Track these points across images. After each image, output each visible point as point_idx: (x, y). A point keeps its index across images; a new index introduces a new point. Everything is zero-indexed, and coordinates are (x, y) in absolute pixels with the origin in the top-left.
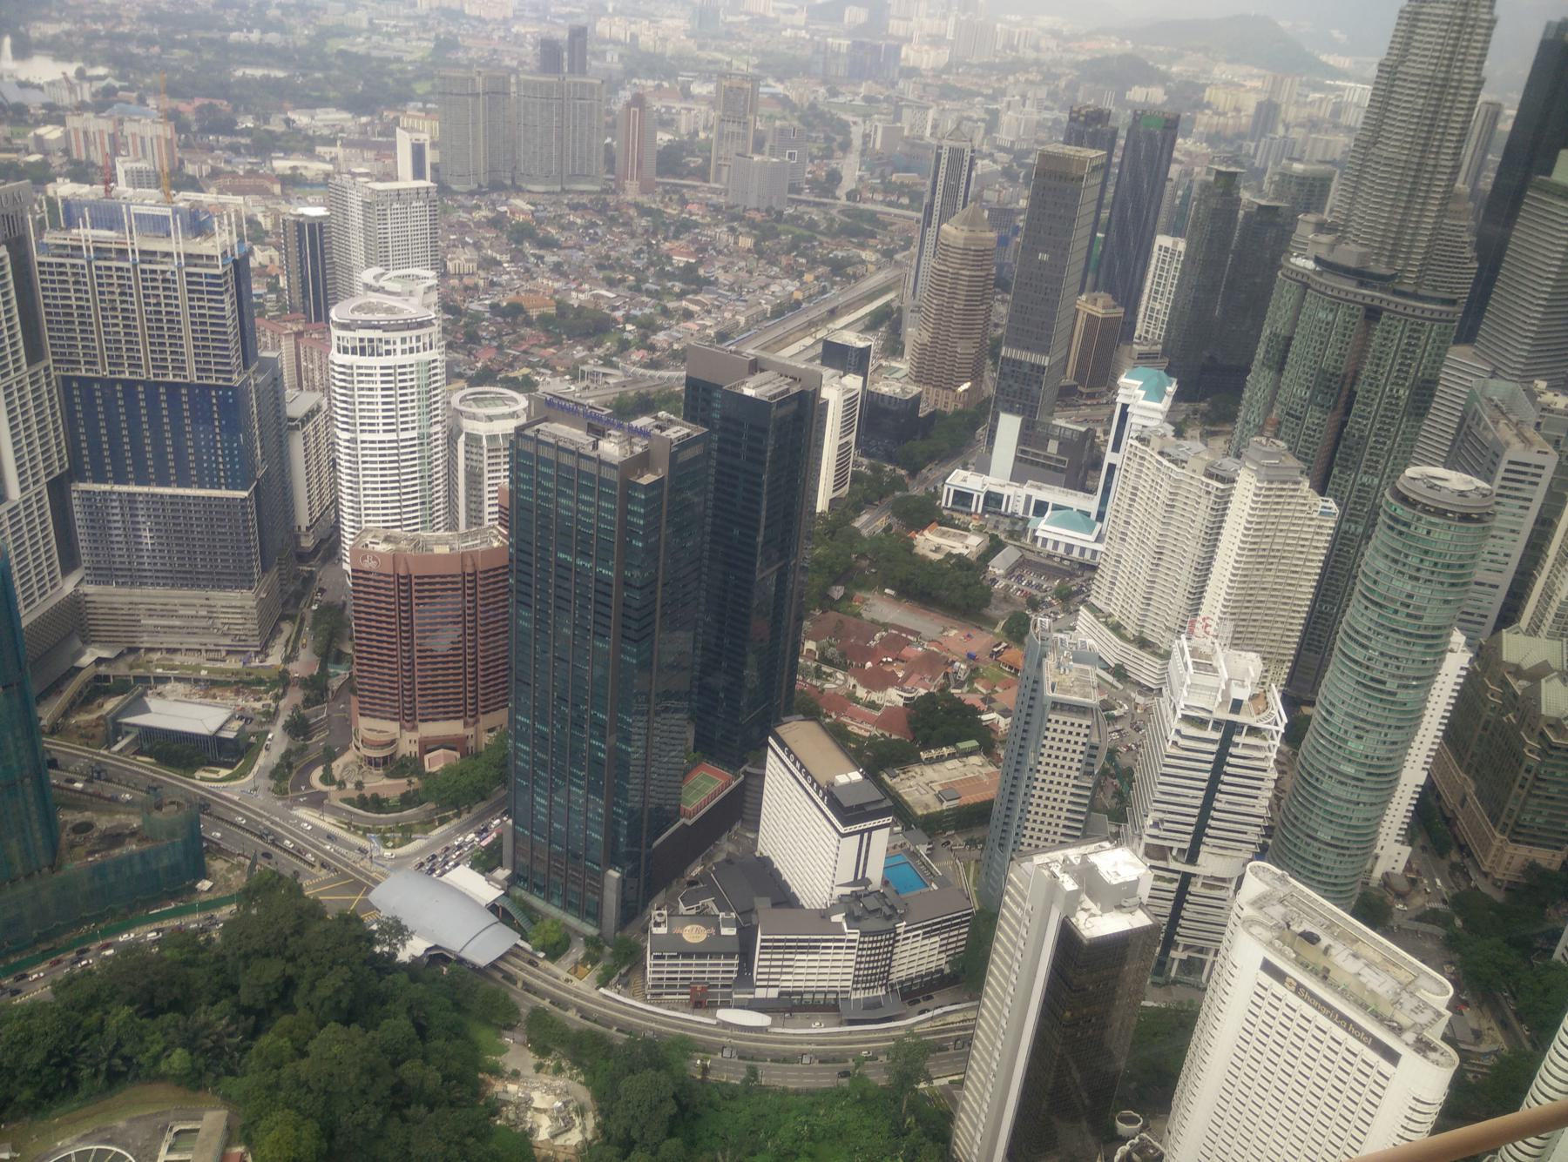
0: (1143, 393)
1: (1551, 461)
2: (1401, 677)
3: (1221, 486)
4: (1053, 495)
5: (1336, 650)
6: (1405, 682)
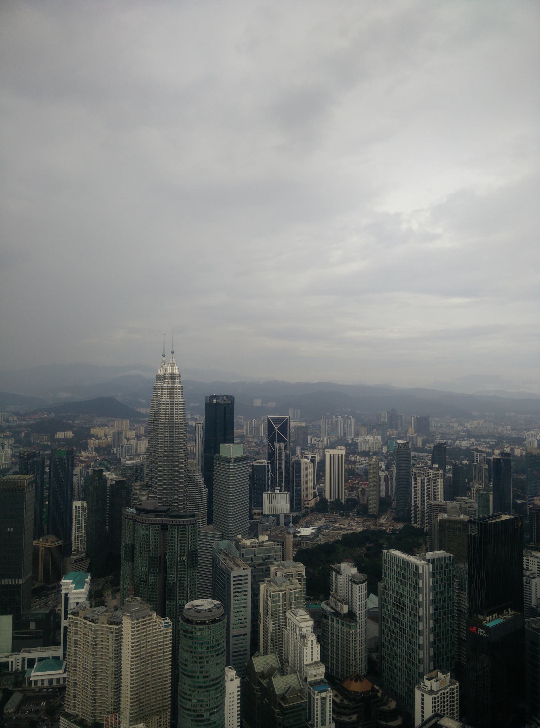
0: (73, 586)
1: (249, 572)
2: (210, 710)
3: (117, 627)
4: (37, 654)
5: (179, 708)
6: (212, 711)
